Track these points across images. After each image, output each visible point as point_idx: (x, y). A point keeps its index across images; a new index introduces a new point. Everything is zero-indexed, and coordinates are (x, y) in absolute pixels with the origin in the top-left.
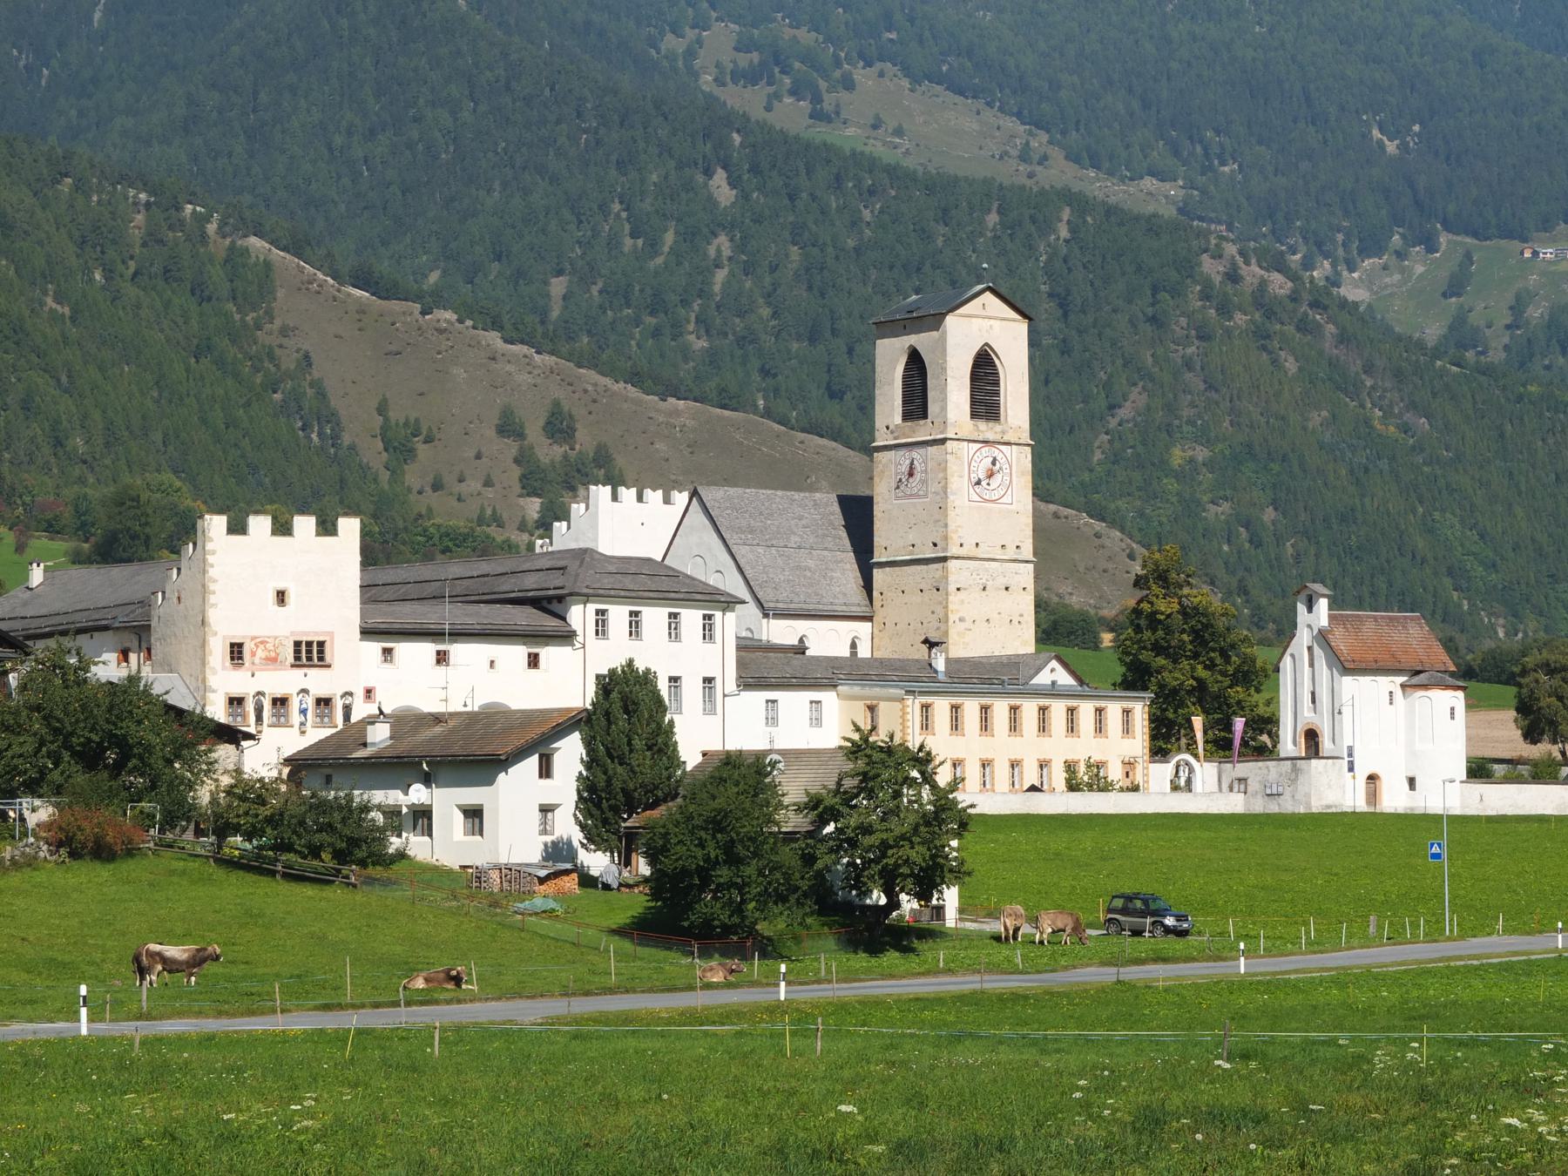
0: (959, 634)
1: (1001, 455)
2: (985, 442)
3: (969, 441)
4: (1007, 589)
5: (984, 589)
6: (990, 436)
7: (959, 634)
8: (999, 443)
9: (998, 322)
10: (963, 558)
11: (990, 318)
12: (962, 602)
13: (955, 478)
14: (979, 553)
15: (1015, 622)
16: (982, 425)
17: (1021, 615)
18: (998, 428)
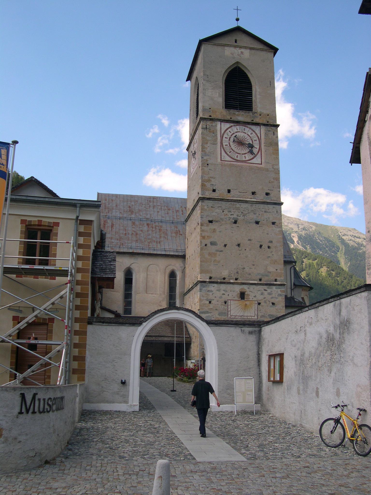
0: (210, 254)
3: (222, 121)
6: (240, 119)
7: (210, 254)
8: (248, 123)
9: (248, 51)
11: (241, 47)
12: (214, 231)
14: (229, 197)
15: (265, 246)
17: (271, 242)
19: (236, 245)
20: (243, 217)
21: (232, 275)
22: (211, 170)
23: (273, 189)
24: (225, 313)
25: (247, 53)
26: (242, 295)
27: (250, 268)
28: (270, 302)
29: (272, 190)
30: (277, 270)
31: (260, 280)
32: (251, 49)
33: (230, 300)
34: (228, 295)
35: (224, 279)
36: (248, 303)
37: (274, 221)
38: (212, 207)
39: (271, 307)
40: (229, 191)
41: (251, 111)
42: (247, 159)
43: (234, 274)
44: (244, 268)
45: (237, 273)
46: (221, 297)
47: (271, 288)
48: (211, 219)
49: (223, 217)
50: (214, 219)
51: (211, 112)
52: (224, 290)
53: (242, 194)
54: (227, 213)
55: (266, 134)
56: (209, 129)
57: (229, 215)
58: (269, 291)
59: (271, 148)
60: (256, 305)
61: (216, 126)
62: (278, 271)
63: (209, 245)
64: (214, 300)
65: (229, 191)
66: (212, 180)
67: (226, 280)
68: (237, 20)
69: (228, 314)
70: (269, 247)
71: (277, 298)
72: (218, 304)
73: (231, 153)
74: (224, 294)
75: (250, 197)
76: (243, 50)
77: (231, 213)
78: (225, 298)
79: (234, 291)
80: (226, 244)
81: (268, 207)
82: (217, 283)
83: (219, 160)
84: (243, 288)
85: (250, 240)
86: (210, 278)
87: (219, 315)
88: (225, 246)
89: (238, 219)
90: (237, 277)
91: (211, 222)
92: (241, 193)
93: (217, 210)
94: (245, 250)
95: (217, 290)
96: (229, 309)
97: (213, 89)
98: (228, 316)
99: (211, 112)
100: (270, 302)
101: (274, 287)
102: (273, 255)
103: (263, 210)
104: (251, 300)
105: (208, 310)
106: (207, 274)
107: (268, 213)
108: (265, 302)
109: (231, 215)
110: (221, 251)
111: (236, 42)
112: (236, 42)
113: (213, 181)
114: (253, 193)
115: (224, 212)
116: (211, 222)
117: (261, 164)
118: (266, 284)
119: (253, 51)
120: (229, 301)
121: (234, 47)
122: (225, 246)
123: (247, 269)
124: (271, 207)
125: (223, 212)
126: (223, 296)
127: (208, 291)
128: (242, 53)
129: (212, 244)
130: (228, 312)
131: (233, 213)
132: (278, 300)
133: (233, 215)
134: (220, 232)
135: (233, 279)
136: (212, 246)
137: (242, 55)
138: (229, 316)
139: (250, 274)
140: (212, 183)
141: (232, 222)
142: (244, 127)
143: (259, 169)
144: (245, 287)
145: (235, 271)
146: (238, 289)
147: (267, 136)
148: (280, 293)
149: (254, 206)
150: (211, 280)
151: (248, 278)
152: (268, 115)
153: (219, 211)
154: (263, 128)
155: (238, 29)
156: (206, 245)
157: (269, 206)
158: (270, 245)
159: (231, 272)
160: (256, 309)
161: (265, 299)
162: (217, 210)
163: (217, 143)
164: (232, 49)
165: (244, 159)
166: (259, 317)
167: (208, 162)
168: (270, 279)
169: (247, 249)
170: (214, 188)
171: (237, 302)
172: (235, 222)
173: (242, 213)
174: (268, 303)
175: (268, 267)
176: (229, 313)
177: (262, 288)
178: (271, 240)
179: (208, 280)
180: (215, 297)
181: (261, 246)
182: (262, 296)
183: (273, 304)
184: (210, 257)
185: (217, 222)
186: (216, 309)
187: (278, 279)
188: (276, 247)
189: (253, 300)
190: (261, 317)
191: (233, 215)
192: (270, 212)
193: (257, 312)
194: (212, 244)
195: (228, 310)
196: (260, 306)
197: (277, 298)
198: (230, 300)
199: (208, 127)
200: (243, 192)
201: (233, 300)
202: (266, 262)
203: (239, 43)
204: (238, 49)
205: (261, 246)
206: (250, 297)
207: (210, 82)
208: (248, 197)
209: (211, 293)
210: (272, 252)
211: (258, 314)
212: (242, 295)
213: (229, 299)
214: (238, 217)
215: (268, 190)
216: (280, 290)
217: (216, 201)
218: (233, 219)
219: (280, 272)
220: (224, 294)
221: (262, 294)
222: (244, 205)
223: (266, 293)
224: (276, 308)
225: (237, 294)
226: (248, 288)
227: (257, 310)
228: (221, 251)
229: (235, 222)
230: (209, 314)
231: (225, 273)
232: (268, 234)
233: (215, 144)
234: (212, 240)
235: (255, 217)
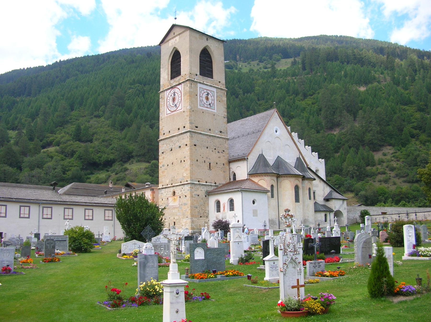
4: (180, 147)
5: (172, 150)
6: (174, 84)
9: (178, 36)
15: (183, 161)
16: (172, 81)
17: (185, 157)
18: (178, 78)
26: (174, 193)
32: (179, 34)
36: (175, 197)
44: (174, 177)
46: (166, 196)
55: (184, 88)
66: (163, 128)
78: (168, 196)
83: (166, 115)
85: (177, 159)
86: (163, 186)
101: (186, 186)
103: (182, 138)
108: (182, 196)
119: (180, 35)
124: (185, 135)
126: (167, 195)
128: (176, 40)
142: (175, 89)
144: (174, 188)
146: (172, 190)
148: (188, 189)
154: (183, 84)
169: (176, 165)
171: (171, 198)
172: (172, 150)
187: (188, 180)
196: (180, 199)
204: (174, 39)
212: (174, 193)
221: (181, 191)
222: (175, 138)
231: (168, 182)
233: (164, 106)
234: (163, 163)
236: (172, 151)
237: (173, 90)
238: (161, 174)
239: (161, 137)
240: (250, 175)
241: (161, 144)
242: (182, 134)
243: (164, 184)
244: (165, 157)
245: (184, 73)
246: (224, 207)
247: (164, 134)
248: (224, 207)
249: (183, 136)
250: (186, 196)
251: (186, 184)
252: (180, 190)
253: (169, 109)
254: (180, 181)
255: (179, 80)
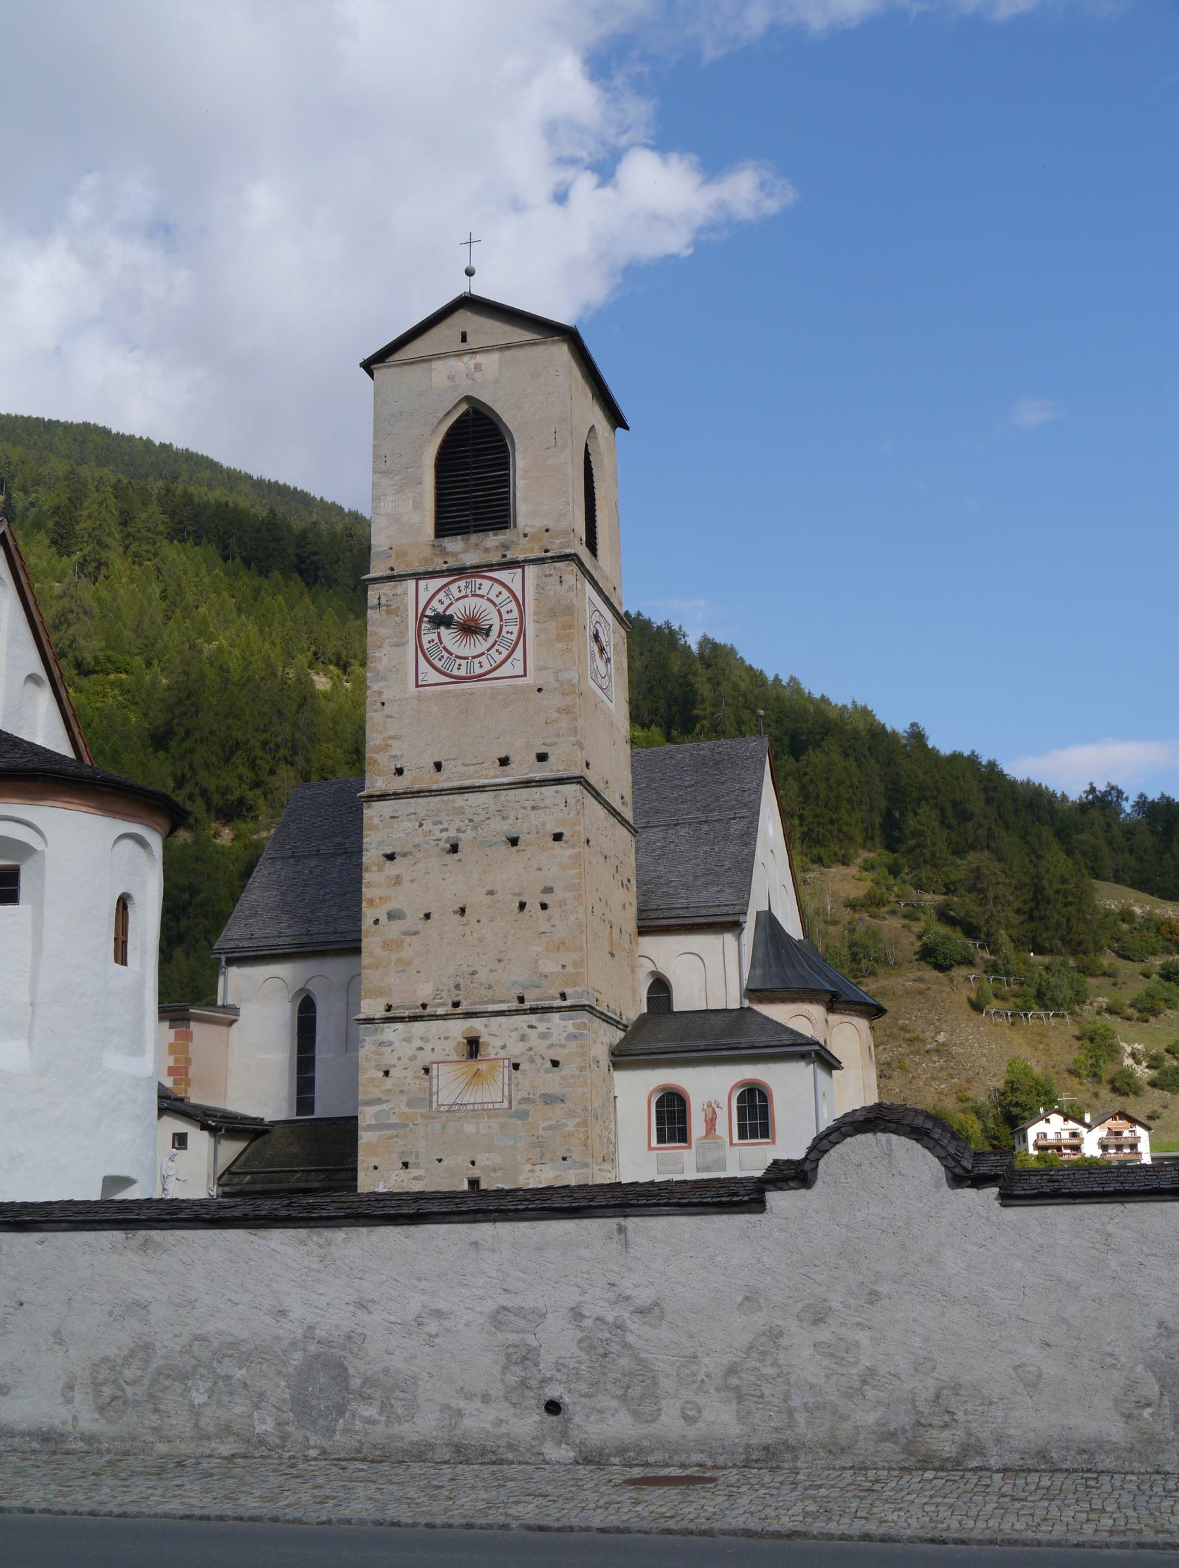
0: (386, 945)
1: (498, 588)
2: (459, 572)
3: (418, 576)
4: (514, 842)
5: (454, 849)
6: (471, 559)
7: (386, 945)
8: (490, 567)
9: (496, 356)
10: (397, 796)
11: (473, 352)
12: (398, 880)
13: (386, 649)
15: (533, 906)
16: (454, 544)
18: (492, 540)
19: (455, 912)
20: (473, 834)
21: (444, 994)
22: (392, 717)
23: (555, 740)
24: (423, 1099)
25: (490, 362)
26: (473, 1046)
27: (491, 971)
28: (543, 1058)
29: (555, 744)
30: (564, 966)
31: (521, 1000)
33: (438, 1063)
34: (433, 1049)
35: (424, 1006)
36: (483, 1067)
37: (557, 831)
38: (392, 818)
39: (547, 1071)
40: (438, 766)
41: (507, 528)
42: (487, 667)
43: (449, 991)
44: (474, 973)
45: (457, 987)
47: (548, 1021)
48: (389, 852)
49: (418, 840)
50: (397, 850)
51: (393, 556)
52: (422, 1039)
53: (471, 768)
54: (431, 827)
55: (540, 588)
56: (387, 606)
57: (437, 833)
58: (542, 1027)
59: (554, 623)
60: (506, 1070)
61: (405, 593)
62: (569, 969)
63: (384, 919)
64: (395, 1066)
65: (438, 766)
66: (393, 743)
67: (429, 1010)
68: (470, 273)
69: (431, 1101)
70: (544, 906)
71: (562, 1046)
72: (406, 1077)
73: (443, 660)
74: (421, 1049)
75: (492, 773)
76: (480, 358)
77: (441, 827)
78: (425, 1058)
79: (446, 1038)
80: (428, 911)
81: (541, 793)
82: (401, 1019)
84: (471, 1028)
85: (491, 893)
86: (389, 1008)
87: (407, 1105)
88: (427, 916)
89: (459, 839)
90: (456, 999)
91: (391, 857)
92: (468, 765)
93: (405, 823)
94: (479, 921)
95: (404, 1040)
96: (435, 1089)
97: (398, 492)
98: (431, 1106)
99: (393, 556)
100: (543, 1058)
102: (553, 926)
103: (529, 804)
104: (492, 1056)
105: (380, 1095)
106: (379, 1000)
107: (540, 811)
108: (532, 1061)
109: (441, 831)
110: (416, 933)
111: (464, 338)
112: (464, 338)
113: (396, 748)
114: (504, 762)
115: (424, 827)
116: (391, 857)
117: (525, 675)
118: (533, 1010)
119: (509, 353)
120: (435, 1066)
121: (456, 356)
122: (427, 916)
123: (483, 975)
125: (421, 825)
126: (420, 1054)
127: (381, 1044)
128: (478, 367)
129: (391, 916)
130: (431, 1095)
131: (445, 826)
132: (566, 1051)
133: (446, 830)
134: (412, 881)
135: (444, 1004)
136: (391, 923)
137: (478, 375)
138: (434, 1105)
139: (490, 987)
140: (394, 753)
141: (443, 849)
142: (479, 581)
143: (522, 690)
144: (477, 1024)
145: (452, 983)
146: (458, 1029)
147: (541, 591)
148: (572, 1030)
149: (502, 798)
150: (390, 1014)
151: (486, 999)
152: (547, 530)
153: (409, 824)
154: (530, 570)
155: (468, 302)
156: (376, 922)
157: (544, 789)
158: (546, 899)
159: (441, 987)
160: (506, 1081)
161: (533, 1053)
162: (407, 824)
163: (408, 641)
164: (452, 362)
165: (478, 671)
166: (514, 1103)
167: (384, 698)
168: (547, 995)
169: (484, 919)
170: (398, 766)
171: (458, 1066)
173: (471, 820)
174: (539, 1061)
175: (539, 962)
176: (435, 1098)
177: (523, 1021)
178: (549, 885)
179: (378, 1015)
180: (399, 1058)
181: (522, 906)
182: (522, 1043)
183: (555, 1064)
184: (386, 953)
185: (404, 855)
186: (402, 1092)
187: (568, 991)
188: (562, 903)
189: (499, 1056)
190: (519, 1103)
191: (446, 830)
192: (546, 807)
193: (510, 1089)
194: (391, 916)
195: (431, 1089)
197: (562, 1046)
198: (438, 1063)
199: (383, 601)
200: (475, 762)
201: (444, 1062)
202: (536, 948)
203: (473, 342)
204: (466, 359)
205: (522, 906)
206: (490, 1050)
207: (391, 473)
208: (487, 775)
209: (389, 1049)
210: (549, 918)
211: (510, 1095)
212: (473, 1046)
213: (434, 1060)
214: (461, 835)
215: (544, 744)
216: (571, 1022)
217: (403, 801)
218: (446, 842)
219: (573, 971)
220: (421, 1049)
221: (523, 1038)
223: (533, 1034)
224: (563, 1073)
225: (454, 1044)
226: (486, 1026)
227: (510, 1085)
228: (416, 933)
229: (454, 849)
230: (384, 1106)
231: (424, 991)
232: (540, 869)
234: (392, 905)
235: (509, 827)
236: (456, 856)
237: (462, 583)
238: (378, 951)
239: (376, 783)
240: (753, 993)
241: (373, 813)
242: (528, 784)
243: (394, 1002)
244: (406, 878)
245: (539, 523)
246: (711, 1123)
247: (400, 772)
248: (711, 1123)
249: (536, 797)
250: (555, 1064)
251: (559, 1009)
252: (515, 1035)
253: (439, 664)
254: (518, 991)
255: (505, 546)
